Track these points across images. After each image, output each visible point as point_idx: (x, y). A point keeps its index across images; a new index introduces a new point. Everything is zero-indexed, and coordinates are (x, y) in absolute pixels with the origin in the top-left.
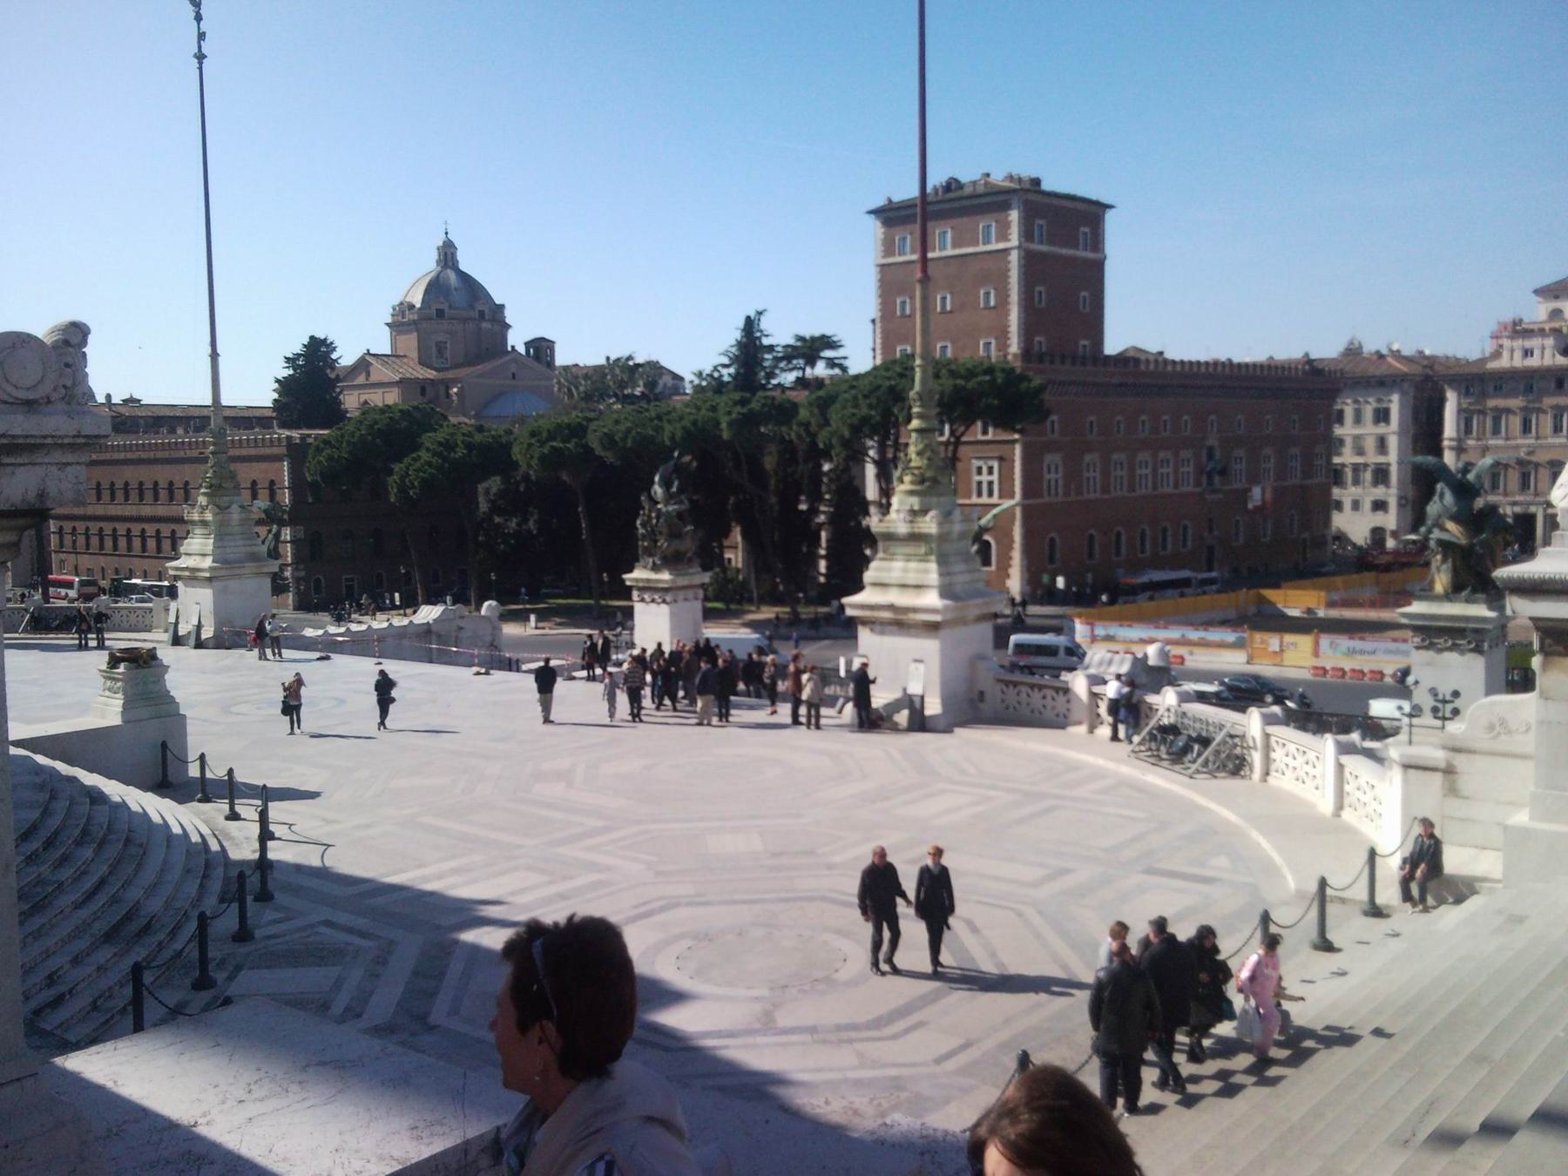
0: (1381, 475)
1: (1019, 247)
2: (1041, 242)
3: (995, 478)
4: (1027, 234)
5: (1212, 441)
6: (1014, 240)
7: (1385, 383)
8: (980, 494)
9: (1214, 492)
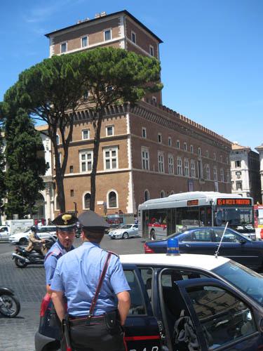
0: (239, 184)
1: (125, 39)
2: (134, 41)
3: (116, 157)
4: (128, 34)
5: (200, 160)
6: (122, 35)
7: (237, 152)
8: (108, 167)
9: (203, 180)
